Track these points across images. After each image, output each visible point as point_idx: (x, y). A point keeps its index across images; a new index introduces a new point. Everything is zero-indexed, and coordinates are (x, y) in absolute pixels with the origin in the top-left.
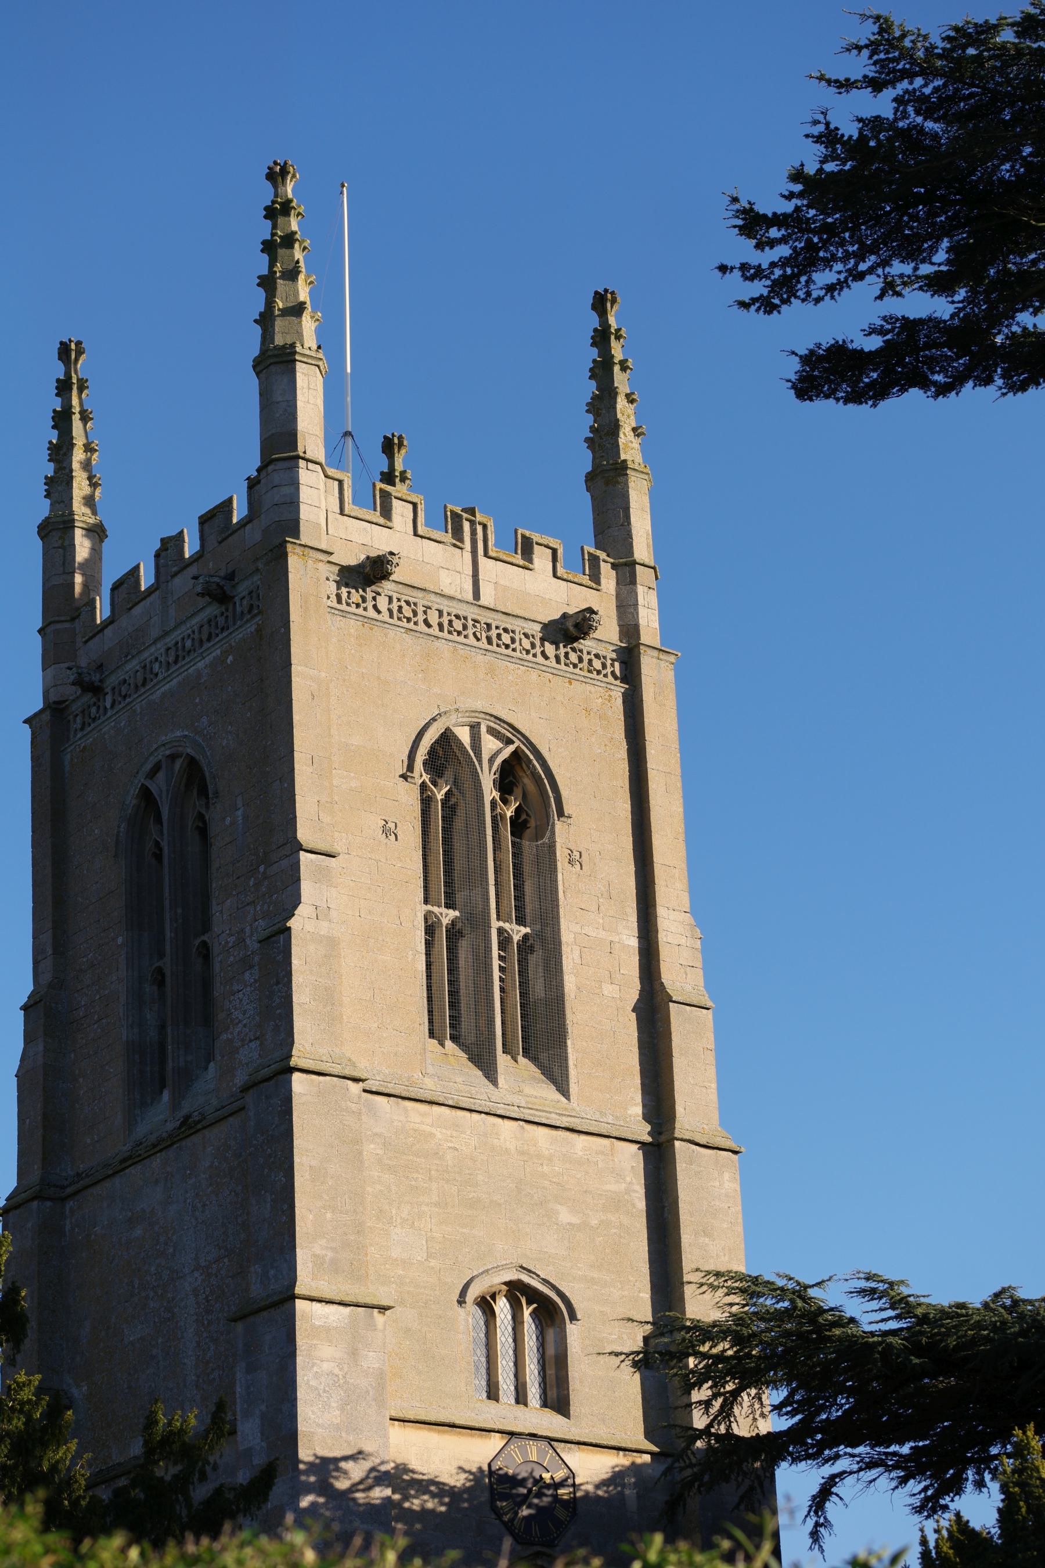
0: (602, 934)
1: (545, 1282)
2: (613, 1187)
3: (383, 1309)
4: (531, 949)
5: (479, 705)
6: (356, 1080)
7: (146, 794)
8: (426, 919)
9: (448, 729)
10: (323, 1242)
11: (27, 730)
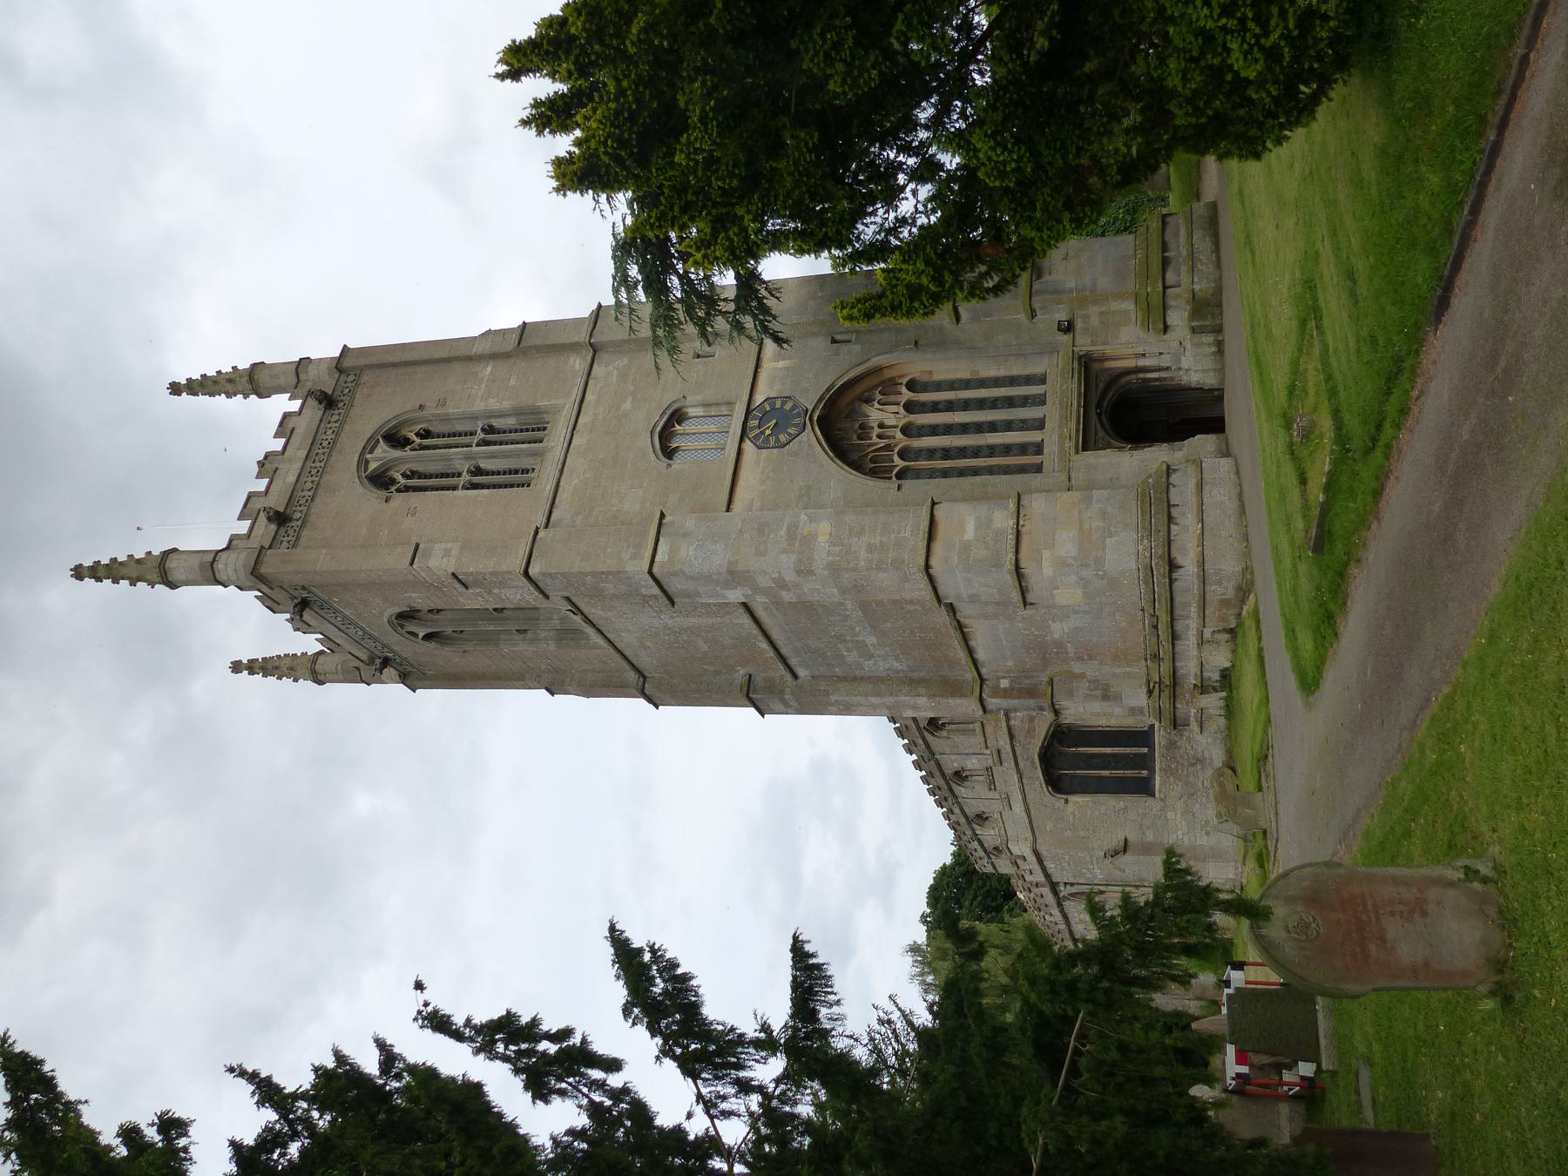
0: (483, 386)
1: (661, 416)
2: (614, 378)
3: (662, 516)
4: (491, 427)
5: (356, 459)
6: (536, 533)
7: (428, 637)
8: (468, 489)
10: (623, 554)
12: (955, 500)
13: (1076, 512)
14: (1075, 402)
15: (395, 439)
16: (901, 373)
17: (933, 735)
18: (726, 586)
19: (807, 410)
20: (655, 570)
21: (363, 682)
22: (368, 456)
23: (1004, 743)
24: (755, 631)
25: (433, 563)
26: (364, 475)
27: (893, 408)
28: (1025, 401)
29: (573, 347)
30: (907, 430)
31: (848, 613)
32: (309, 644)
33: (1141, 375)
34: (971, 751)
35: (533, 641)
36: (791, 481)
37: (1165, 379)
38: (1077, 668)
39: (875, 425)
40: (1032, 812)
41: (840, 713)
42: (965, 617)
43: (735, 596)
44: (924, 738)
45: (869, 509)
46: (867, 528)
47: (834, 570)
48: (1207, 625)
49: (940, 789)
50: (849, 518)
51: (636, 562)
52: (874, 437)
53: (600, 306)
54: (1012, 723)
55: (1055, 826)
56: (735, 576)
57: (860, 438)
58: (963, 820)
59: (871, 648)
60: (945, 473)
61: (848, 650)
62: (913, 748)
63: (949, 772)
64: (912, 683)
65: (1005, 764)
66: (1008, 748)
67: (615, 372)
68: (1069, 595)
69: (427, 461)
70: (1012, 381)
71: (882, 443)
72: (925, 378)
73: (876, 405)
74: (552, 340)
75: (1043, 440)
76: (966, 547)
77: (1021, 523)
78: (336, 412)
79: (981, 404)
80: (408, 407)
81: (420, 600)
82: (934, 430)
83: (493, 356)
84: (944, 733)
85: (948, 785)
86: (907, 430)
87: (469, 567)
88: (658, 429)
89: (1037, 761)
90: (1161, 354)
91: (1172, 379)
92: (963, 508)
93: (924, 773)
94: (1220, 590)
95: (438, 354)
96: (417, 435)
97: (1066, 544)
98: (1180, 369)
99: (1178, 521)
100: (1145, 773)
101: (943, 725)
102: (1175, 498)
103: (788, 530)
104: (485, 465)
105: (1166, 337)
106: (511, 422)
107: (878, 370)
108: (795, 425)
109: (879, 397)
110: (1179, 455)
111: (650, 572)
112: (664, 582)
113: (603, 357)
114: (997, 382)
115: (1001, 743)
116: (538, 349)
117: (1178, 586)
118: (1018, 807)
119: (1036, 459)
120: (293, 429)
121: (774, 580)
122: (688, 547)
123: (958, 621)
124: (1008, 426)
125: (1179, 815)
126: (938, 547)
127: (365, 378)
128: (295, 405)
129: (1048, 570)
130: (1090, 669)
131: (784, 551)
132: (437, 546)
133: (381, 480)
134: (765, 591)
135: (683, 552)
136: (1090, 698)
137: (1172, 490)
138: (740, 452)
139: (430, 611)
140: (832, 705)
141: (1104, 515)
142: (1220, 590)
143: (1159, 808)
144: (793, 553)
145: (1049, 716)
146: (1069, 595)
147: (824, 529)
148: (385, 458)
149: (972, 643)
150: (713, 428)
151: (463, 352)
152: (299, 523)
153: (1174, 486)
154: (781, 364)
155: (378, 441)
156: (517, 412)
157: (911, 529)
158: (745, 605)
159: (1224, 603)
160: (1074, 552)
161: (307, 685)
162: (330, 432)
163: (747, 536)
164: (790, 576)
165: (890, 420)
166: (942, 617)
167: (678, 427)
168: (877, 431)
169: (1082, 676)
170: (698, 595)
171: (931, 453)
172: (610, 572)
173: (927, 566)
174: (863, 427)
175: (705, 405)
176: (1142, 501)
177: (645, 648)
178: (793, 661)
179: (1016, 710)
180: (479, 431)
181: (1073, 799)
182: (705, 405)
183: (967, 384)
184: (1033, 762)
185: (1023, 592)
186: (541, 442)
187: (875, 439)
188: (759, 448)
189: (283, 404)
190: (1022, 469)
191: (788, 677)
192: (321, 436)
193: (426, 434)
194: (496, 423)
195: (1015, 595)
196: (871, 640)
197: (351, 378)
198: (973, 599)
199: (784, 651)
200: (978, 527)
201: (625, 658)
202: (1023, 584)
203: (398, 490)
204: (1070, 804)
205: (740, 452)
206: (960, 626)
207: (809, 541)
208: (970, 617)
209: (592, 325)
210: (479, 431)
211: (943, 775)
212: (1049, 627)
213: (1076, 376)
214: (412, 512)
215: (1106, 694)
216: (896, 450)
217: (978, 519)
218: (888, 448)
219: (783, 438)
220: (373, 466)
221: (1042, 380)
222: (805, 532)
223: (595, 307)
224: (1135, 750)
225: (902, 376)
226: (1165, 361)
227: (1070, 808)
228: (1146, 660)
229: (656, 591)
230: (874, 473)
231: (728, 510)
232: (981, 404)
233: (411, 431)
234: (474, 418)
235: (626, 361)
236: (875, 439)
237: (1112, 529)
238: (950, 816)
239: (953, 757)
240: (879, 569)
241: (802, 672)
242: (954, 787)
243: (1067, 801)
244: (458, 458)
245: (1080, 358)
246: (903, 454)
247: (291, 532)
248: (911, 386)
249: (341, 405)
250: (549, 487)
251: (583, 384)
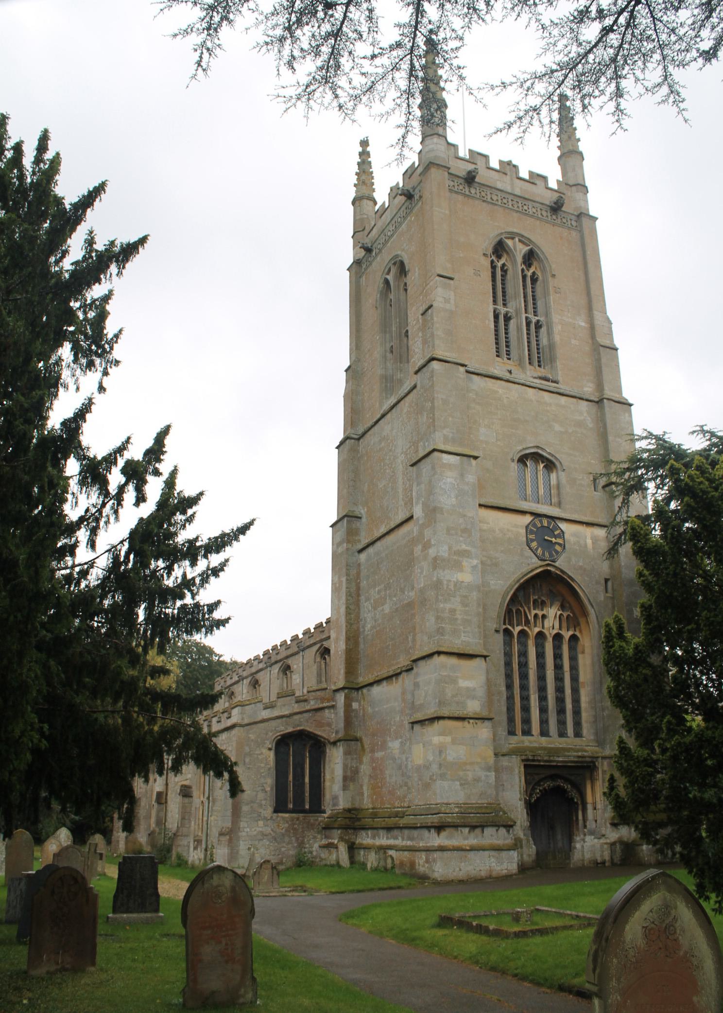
0: (570, 320)
1: (550, 454)
3: (476, 458)
4: (541, 327)
5: (515, 230)
6: (463, 365)
7: (387, 282)
8: (494, 311)
9: (501, 239)
10: (448, 429)
11: (348, 273)
12: (488, 672)
13: (479, 760)
14: (561, 759)
15: (530, 257)
16: (583, 632)
17: (318, 651)
18: (425, 506)
19: (555, 562)
20: (436, 454)
21: (354, 233)
22: (517, 239)
23: (312, 705)
24: (393, 525)
25: (440, 290)
26: (503, 237)
27: (557, 625)
28: (562, 723)
29: (600, 386)
30: (541, 635)
31: (406, 593)
32: (382, 196)
33: (580, 807)
34: (306, 679)
35: (385, 357)
36: (502, 552)
37: (578, 824)
38: (366, 759)
39: (544, 612)
40: (262, 724)
41: (333, 584)
42: (403, 678)
43: (418, 511)
44: (315, 644)
45: (481, 610)
46: (467, 609)
47: (437, 585)
48: (398, 852)
49: (277, 654)
50: (475, 595)
51: (442, 439)
52: (536, 611)
53: (631, 405)
54: (327, 711)
55: (252, 740)
56: (432, 512)
57: (535, 601)
58: (254, 670)
59: (381, 608)
60: (508, 664)
61: (379, 592)
62: (307, 636)
63: (290, 661)
64: (353, 638)
65: (296, 705)
66: (308, 708)
67: (582, 418)
68: (419, 755)
69: (514, 283)
70: (577, 712)
71: (531, 618)
72: (579, 649)
73: (559, 613)
74: (605, 371)
75: (533, 735)
76: (454, 681)
77: (471, 721)
78: (549, 214)
79: (560, 690)
80: (553, 266)
81: (413, 278)
82: (540, 655)
83: (592, 328)
84: (318, 659)
85: (280, 661)
86: (541, 635)
87: (437, 318)
88: (540, 451)
89: (298, 728)
90: (596, 821)
91: (578, 829)
92: (483, 678)
93: (289, 642)
94: (421, 862)
95: (593, 287)
96: (534, 273)
97: (455, 753)
98: (585, 835)
99: (472, 835)
100: (291, 806)
101: (325, 659)
102: (489, 831)
103: (465, 551)
104: (512, 324)
105: (609, 825)
106: (544, 341)
107: (585, 614)
108: (543, 554)
109: (565, 614)
110: (521, 835)
111: (434, 450)
112: (428, 460)
113: (594, 408)
114: (576, 701)
115: (312, 703)
116: (599, 360)
117: (425, 833)
118: (266, 714)
119: (519, 731)
120: (535, 184)
121: (429, 540)
122: (452, 478)
123: (400, 673)
124: (543, 710)
125: (261, 829)
126: (453, 661)
127: (574, 233)
128: (553, 184)
129: (436, 740)
130: (365, 769)
131: (450, 548)
132: (452, 293)
133: (500, 249)
134: (421, 534)
135: (449, 474)
136: (345, 767)
137: (494, 829)
138: (523, 512)
139: (406, 284)
140: (339, 578)
141: (477, 780)
142: (421, 862)
143: (266, 815)
144: (449, 555)
145: (333, 737)
146: (419, 755)
147: (466, 577)
148: (516, 251)
149: (385, 683)
150: (541, 491)
151: (595, 305)
152: (467, 193)
153: (497, 830)
154: (589, 542)
155: (528, 245)
156: (552, 346)
157: (468, 640)
158: (411, 517)
159: (413, 864)
160: (450, 758)
161: (352, 193)
162: (534, 210)
163: (461, 520)
164: (432, 552)
165: (548, 623)
166: (403, 661)
167: (542, 466)
168: (540, 613)
169: (361, 762)
170: (418, 484)
171: (523, 654)
172: (434, 420)
173: (439, 653)
174: (543, 603)
175: (558, 486)
176: (486, 807)
177: (380, 442)
178: (371, 550)
179: (336, 714)
180: (537, 318)
181: (271, 755)
182: (558, 486)
183: (575, 679)
184: (298, 726)
185: (421, 722)
186: (530, 363)
187: (533, 612)
188: (527, 527)
189: (554, 175)
190: (511, 720)
191: (360, 547)
192: (530, 203)
193: (534, 280)
194: (543, 330)
195: (419, 716)
196: (387, 608)
197: (574, 224)
198: (416, 685)
199: (378, 544)
200: (468, 689)
201: (373, 426)
202: (427, 722)
203: (492, 262)
204: (268, 752)
205: (523, 512)
206: (397, 675)
207: (458, 566)
208: (403, 682)
209: (617, 399)
210: (537, 318)
211: (287, 657)
212: (397, 738)
213: (580, 759)
214: (477, 273)
215: (350, 778)
216: (526, 628)
217: (474, 689)
218: (527, 622)
219: (534, 545)
220: (510, 242)
221: (578, 734)
222: (464, 563)
223: (631, 401)
224: (307, 799)
225: (581, 632)
226: (591, 824)
227: (265, 751)
228: (373, 808)
229: (421, 454)
230: (509, 611)
231: (480, 505)
232: (560, 690)
233: (536, 268)
234: (547, 314)
235: (591, 425)
236: (533, 612)
237: (466, 786)
238: (257, 661)
239: (301, 665)
240: (438, 618)
241: (363, 556)
242: (279, 665)
243: (270, 749)
244: (516, 304)
245: (594, 763)
246: (523, 633)
247: (461, 187)
248: (574, 639)
249: (554, 217)
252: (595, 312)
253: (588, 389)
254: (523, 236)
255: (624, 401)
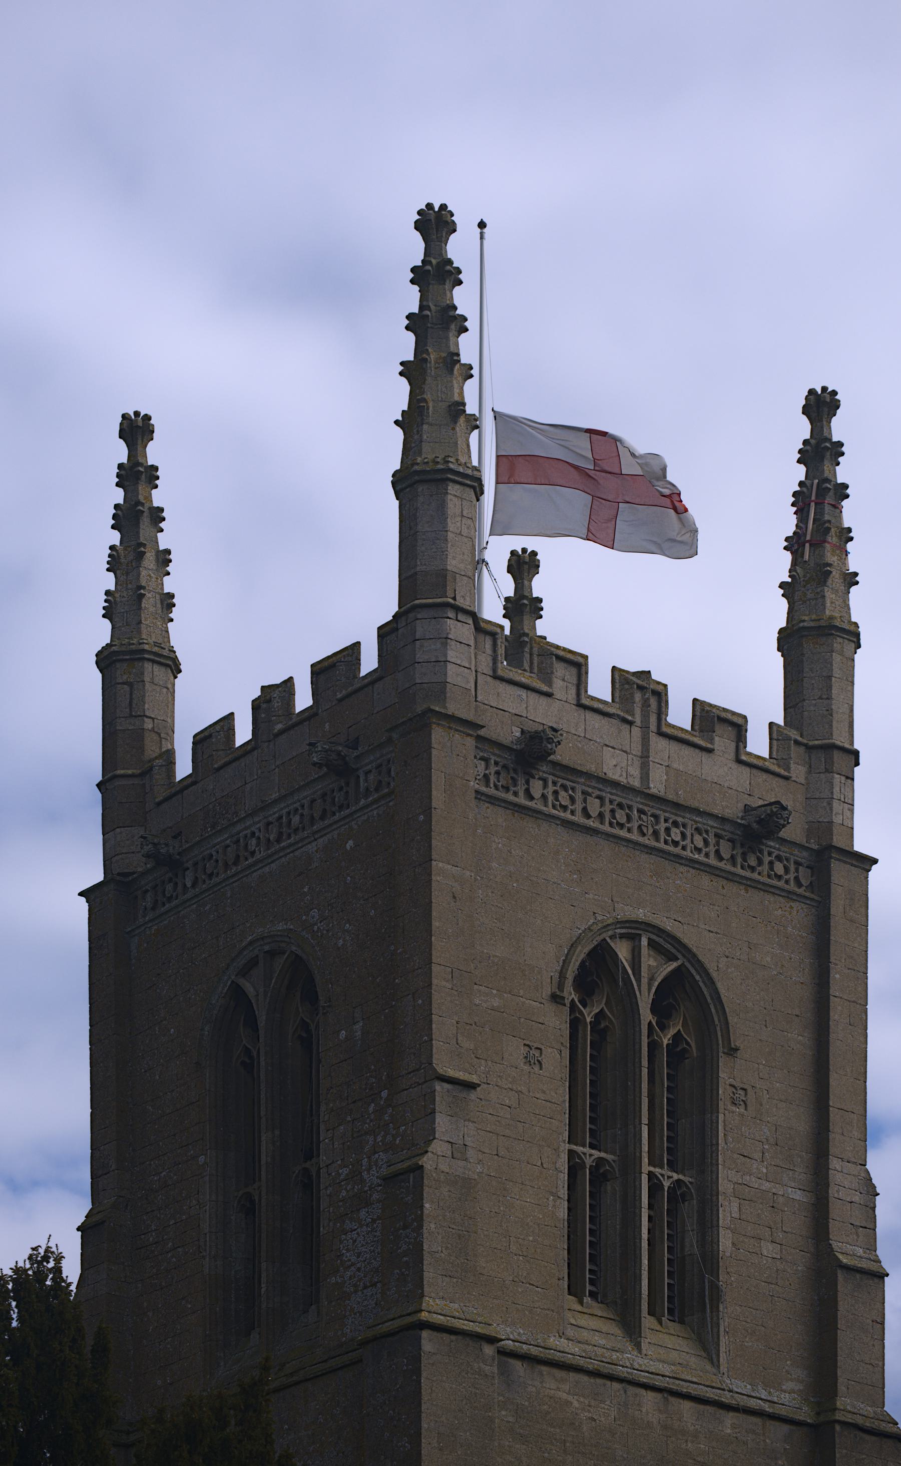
0: (766, 1186)
5: (641, 914)
22: (644, 942)
96: (677, 1037)
148: (639, 981)
151: (837, 1142)
214: (534, 1060)
233: (685, 1024)
250: (562, 1344)
251: (753, 1403)
252: (834, 1163)
253: (805, 1414)
254: (660, 931)
255: (890, 1428)
